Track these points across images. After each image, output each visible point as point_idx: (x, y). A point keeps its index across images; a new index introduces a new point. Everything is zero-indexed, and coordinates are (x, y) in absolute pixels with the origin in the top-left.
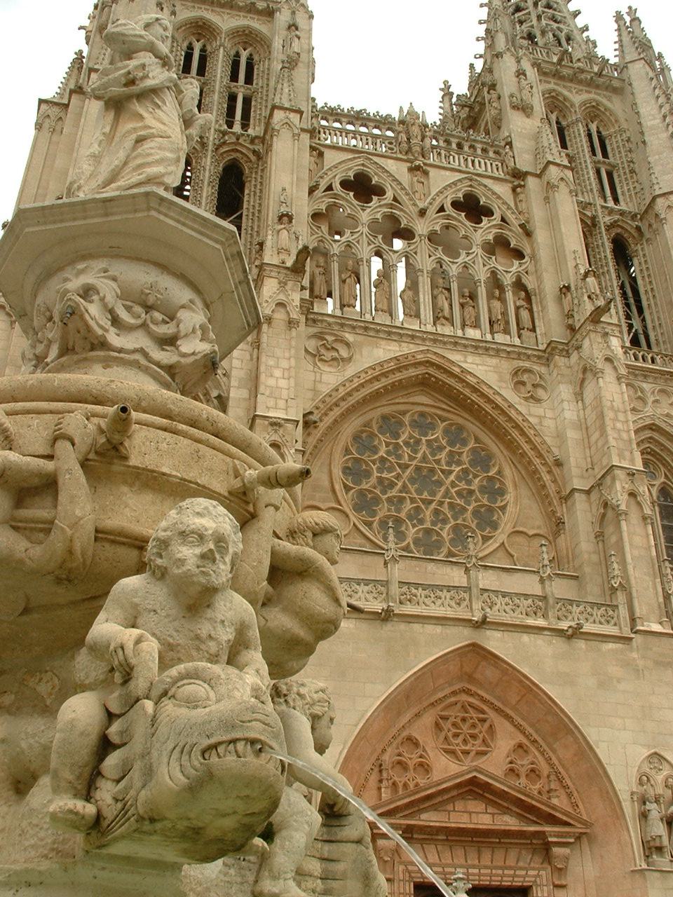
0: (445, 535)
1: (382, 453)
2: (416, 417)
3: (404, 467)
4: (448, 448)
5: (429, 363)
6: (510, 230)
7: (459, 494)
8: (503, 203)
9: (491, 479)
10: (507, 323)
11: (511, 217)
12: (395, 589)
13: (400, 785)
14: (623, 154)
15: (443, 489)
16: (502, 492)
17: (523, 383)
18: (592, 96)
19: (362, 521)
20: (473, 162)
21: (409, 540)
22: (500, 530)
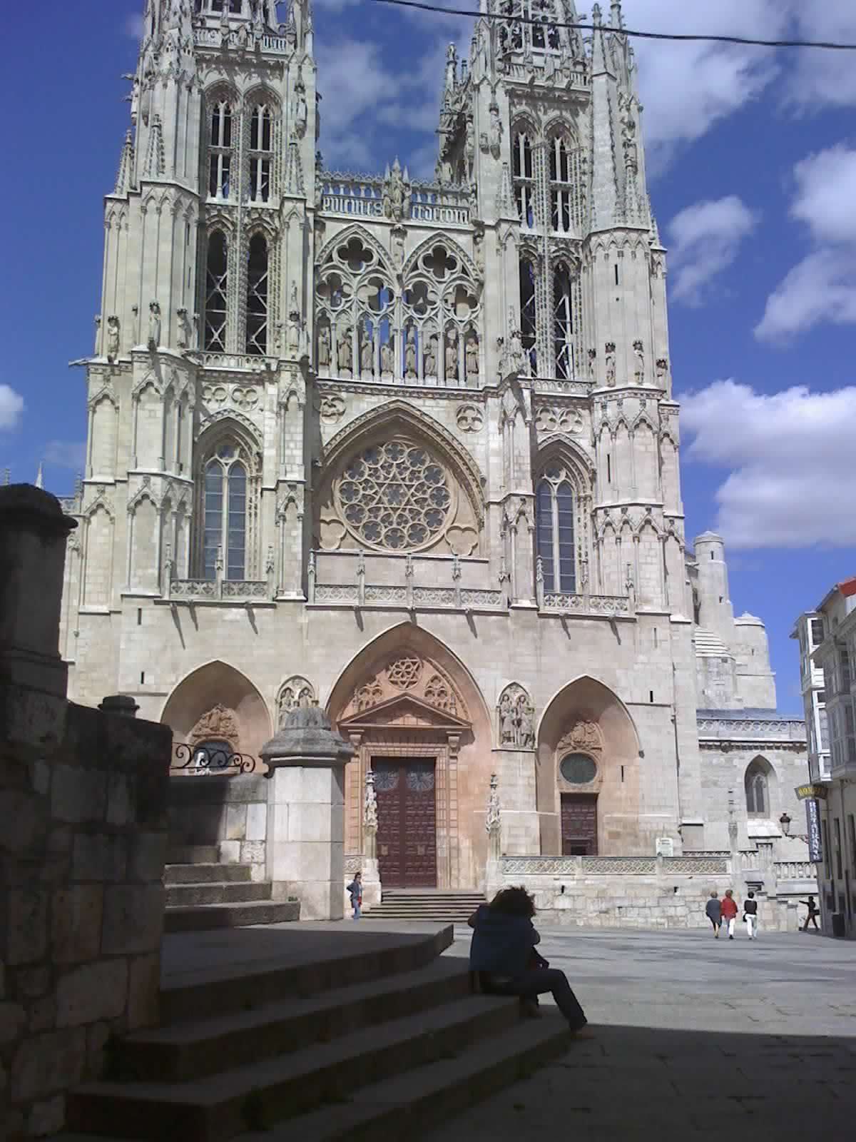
0: (405, 531)
1: (366, 477)
3: (380, 485)
4: (411, 468)
5: (399, 410)
6: (468, 281)
8: (464, 256)
9: (439, 489)
10: (457, 371)
11: (470, 268)
13: (365, 703)
15: (406, 499)
16: (447, 497)
17: (465, 418)
18: (557, 113)
19: (354, 527)
21: (382, 537)
22: (442, 526)
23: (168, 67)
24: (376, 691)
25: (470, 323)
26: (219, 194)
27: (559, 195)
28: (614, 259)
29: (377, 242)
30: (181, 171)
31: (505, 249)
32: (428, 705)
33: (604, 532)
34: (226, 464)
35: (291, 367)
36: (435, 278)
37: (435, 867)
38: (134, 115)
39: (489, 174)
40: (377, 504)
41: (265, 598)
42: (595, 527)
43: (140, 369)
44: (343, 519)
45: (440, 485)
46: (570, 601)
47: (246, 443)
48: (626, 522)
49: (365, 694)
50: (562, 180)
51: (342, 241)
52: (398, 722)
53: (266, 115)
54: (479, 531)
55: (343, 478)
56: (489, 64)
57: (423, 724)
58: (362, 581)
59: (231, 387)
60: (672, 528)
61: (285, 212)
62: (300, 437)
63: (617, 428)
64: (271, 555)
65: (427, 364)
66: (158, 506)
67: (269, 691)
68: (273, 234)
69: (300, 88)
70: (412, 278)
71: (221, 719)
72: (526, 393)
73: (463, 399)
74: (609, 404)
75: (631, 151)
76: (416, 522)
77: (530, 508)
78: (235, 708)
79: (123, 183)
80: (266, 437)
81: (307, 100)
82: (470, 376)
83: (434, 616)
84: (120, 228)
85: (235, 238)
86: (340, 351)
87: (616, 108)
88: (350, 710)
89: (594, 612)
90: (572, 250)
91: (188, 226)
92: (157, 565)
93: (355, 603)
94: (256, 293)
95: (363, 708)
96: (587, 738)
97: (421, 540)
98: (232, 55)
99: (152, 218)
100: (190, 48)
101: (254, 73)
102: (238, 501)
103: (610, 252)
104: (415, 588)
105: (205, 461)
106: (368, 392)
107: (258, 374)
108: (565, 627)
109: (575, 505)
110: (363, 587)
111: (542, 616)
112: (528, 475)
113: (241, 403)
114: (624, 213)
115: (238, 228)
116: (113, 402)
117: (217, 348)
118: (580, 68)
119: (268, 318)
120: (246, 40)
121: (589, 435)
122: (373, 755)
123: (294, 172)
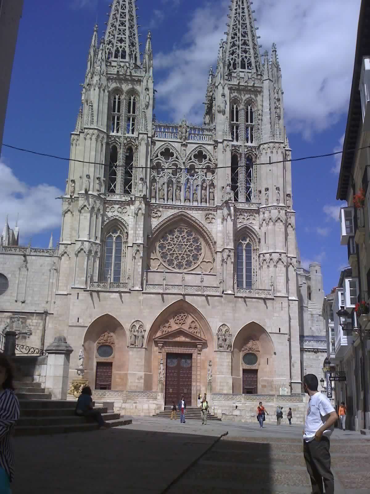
0: (184, 263)
1: (169, 241)
2: (179, 229)
4: (187, 238)
6: (211, 164)
9: (198, 246)
11: (212, 159)
14: (257, 120)
15: (185, 250)
16: (201, 249)
17: (209, 218)
18: (249, 96)
20: (202, 137)
21: (175, 265)
23: (96, 82)
24: (169, 327)
25: (212, 180)
26: (115, 131)
27: (249, 128)
28: (269, 154)
30: (100, 123)
31: (226, 151)
32: (190, 333)
33: (263, 263)
34: (115, 236)
35: (139, 199)
37: (191, 397)
38: (83, 101)
39: (221, 122)
40: (173, 252)
41: (126, 289)
42: (259, 261)
43: (82, 200)
44: (159, 258)
45: (198, 244)
47: (122, 228)
48: (271, 259)
49: (165, 328)
50: (251, 123)
51: (162, 149)
52: (178, 339)
53: (134, 100)
54: (213, 263)
55: (160, 241)
56: (222, 77)
57: (188, 340)
58: (165, 283)
60: (291, 262)
61: (139, 139)
62: (142, 226)
63: (269, 222)
64: (129, 272)
65: (194, 197)
66: (87, 253)
67: (127, 326)
68: (136, 146)
69: (147, 89)
70: (189, 163)
71: (108, 337)
72: (232, 208)
74: (266, 212)
75: (278, 111)
76: (188, 259)
77: (232, 254)
78: (114, 332)
79: (78, 128)
80: (130, 226)
81: (150, 94)
82: (211, 201)
83: (192, 297)
84: (76, 145)
85: (120, 148)
86: (160, 192)
87: (272, 94)
88: (159, 334)
89: (257, 296)
90: (254, 150)
91: (102, 145)
92: (85, 276)
93: (161, 291)
94: (129, 170)
95: (164, 333)
96: (254, 347)
97: (190, 266)
98: (122, 77)
99: (88, 141)
100: (105, 74)
101: (130, 83)
102: (119, 251)
103: (268, 151)
104: (185, 286)
105: (106, 235)
106: (171, 208)
107: (127, 201)
108: (245, 301)
109: (252, 251)
110: (165, 285)
111: (236, 297)
112: (232, 241)
113: (121, 213)
114: (274, 135)
115: (122, 145)
116: (72, 213)
117: (113, 191)
118: (259, 77)
119: (133, 180)
120: (126, 71)
121: (258, 224)
122: (167, 351)
123: (144, 123)
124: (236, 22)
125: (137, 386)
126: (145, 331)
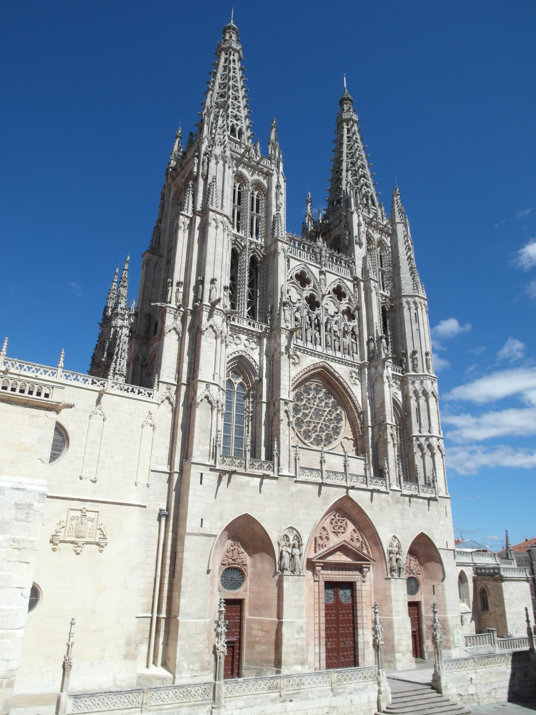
3: (311, 408)
5: (324, 367)
7: (328, 420)
9: (338, 414)
11: (353, 299)
12: (325, 474)
15: (323, 418)
16: (341, 419)
21: (312, 440)
28: (413, 311)
29: (314, 275)
36: (338, 301)
46: (413, 487)
59: (244, 337)
67: (274, 536)
69: (278, 187)
73: (352, 367)
76: (327, 432)
83: (358, 491)
89: (422, 495)
93: (320, 481)
97: (330, 442)
111: (402, 495)
124: (349, 150)
125: (297, 645)
126: (302, 545)
